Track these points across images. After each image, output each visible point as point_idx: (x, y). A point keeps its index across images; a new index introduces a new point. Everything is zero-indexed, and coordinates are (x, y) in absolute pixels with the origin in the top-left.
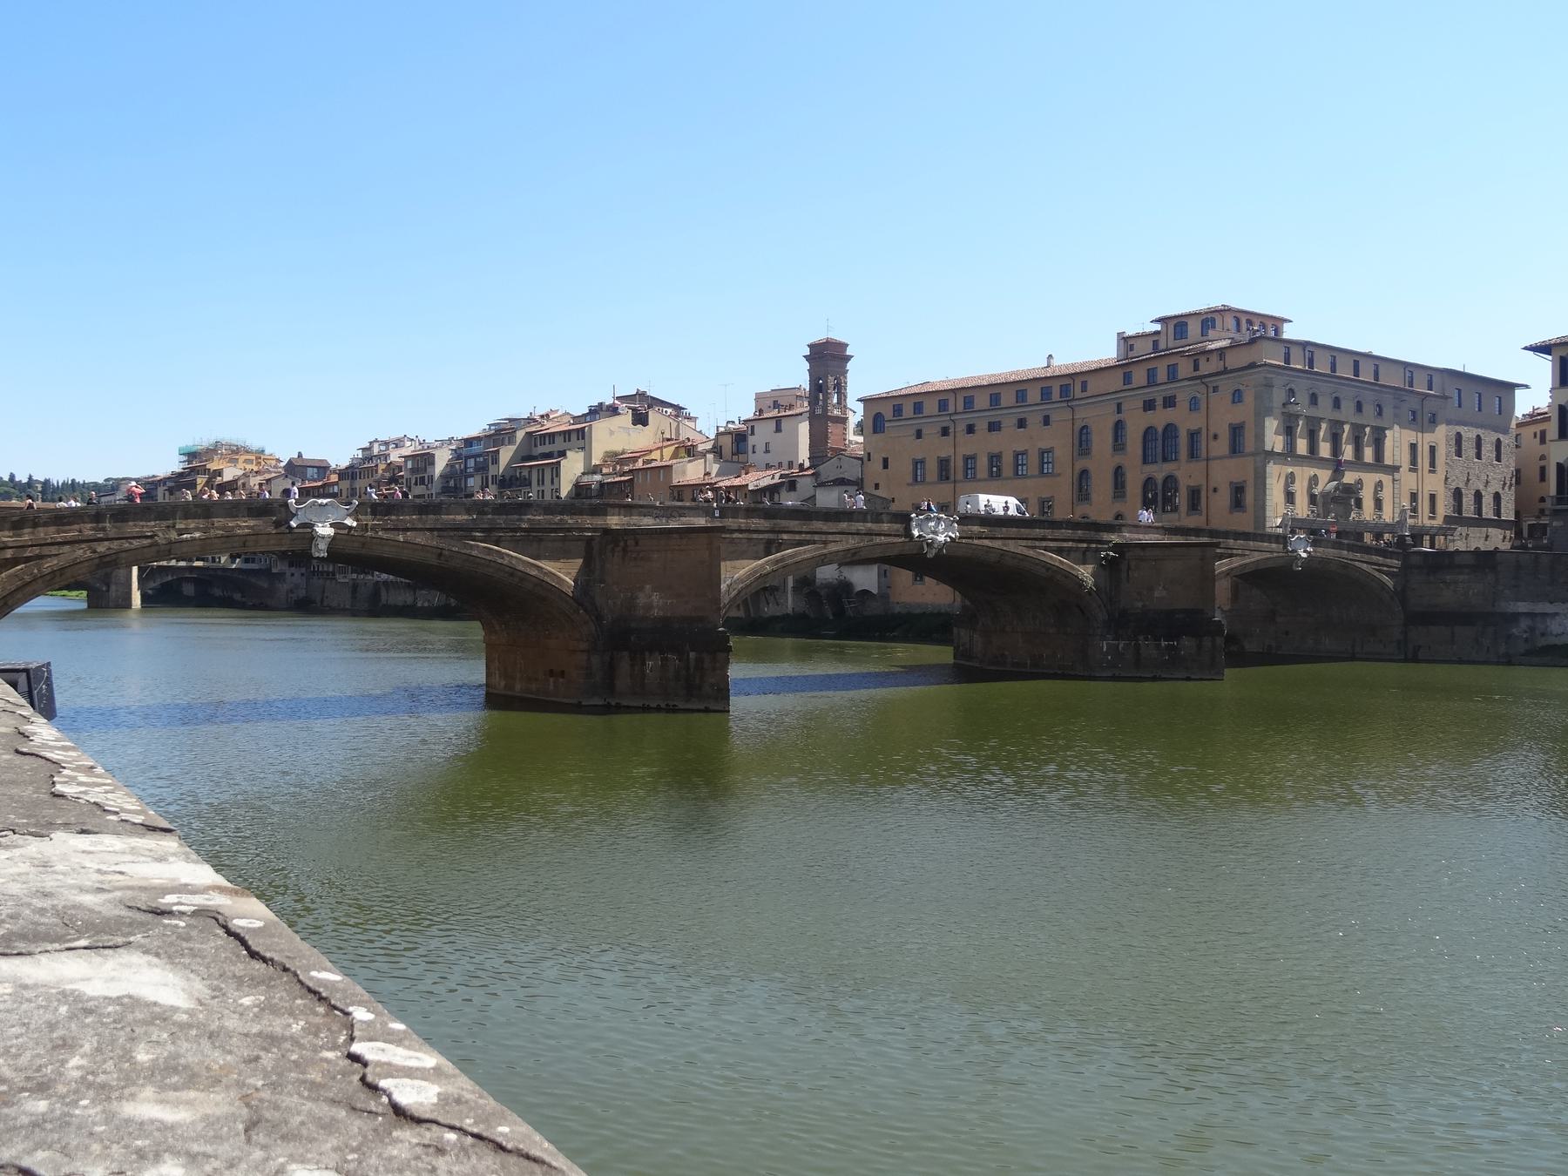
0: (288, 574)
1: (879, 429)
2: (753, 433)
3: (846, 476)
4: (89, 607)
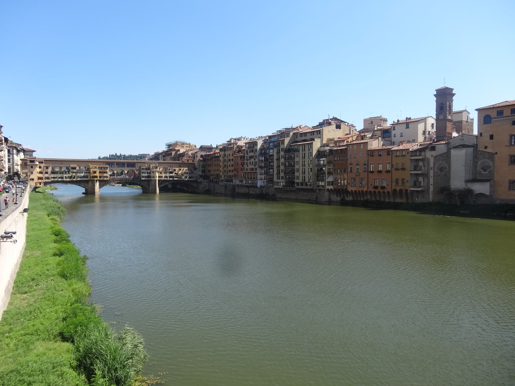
2: (394, 129)
4: (143, 193)
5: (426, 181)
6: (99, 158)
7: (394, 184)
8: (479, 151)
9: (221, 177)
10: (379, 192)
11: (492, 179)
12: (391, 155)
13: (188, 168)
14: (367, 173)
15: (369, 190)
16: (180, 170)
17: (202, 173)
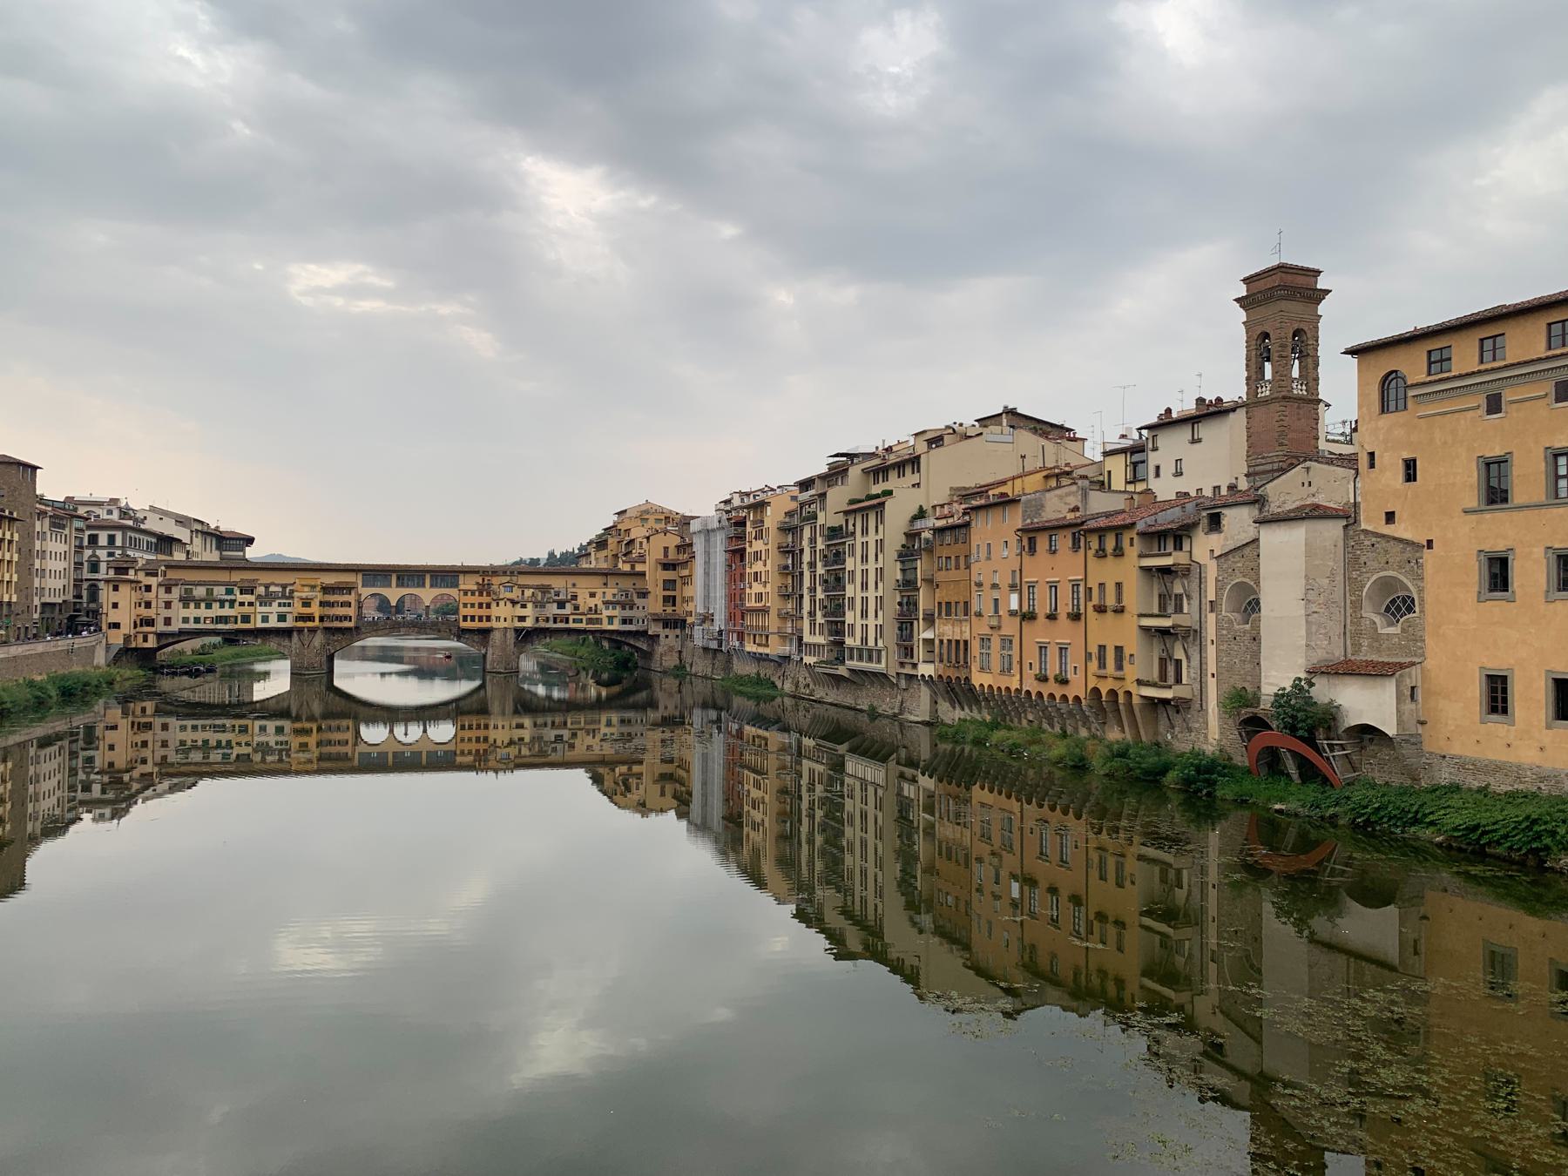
0: (662, 638)
1: (1392, 405)
2: (1155, 449)
3: (1320, 500)
5: (1195, 662)
6: (552, 555)
7: (1093, 666)
8: (1366, 532)
10: (1052, 696)
11: (1413, 664)
12: (1082, 550)
14: (1018, 619)
15: (1025, 689)
16: (593, 595)
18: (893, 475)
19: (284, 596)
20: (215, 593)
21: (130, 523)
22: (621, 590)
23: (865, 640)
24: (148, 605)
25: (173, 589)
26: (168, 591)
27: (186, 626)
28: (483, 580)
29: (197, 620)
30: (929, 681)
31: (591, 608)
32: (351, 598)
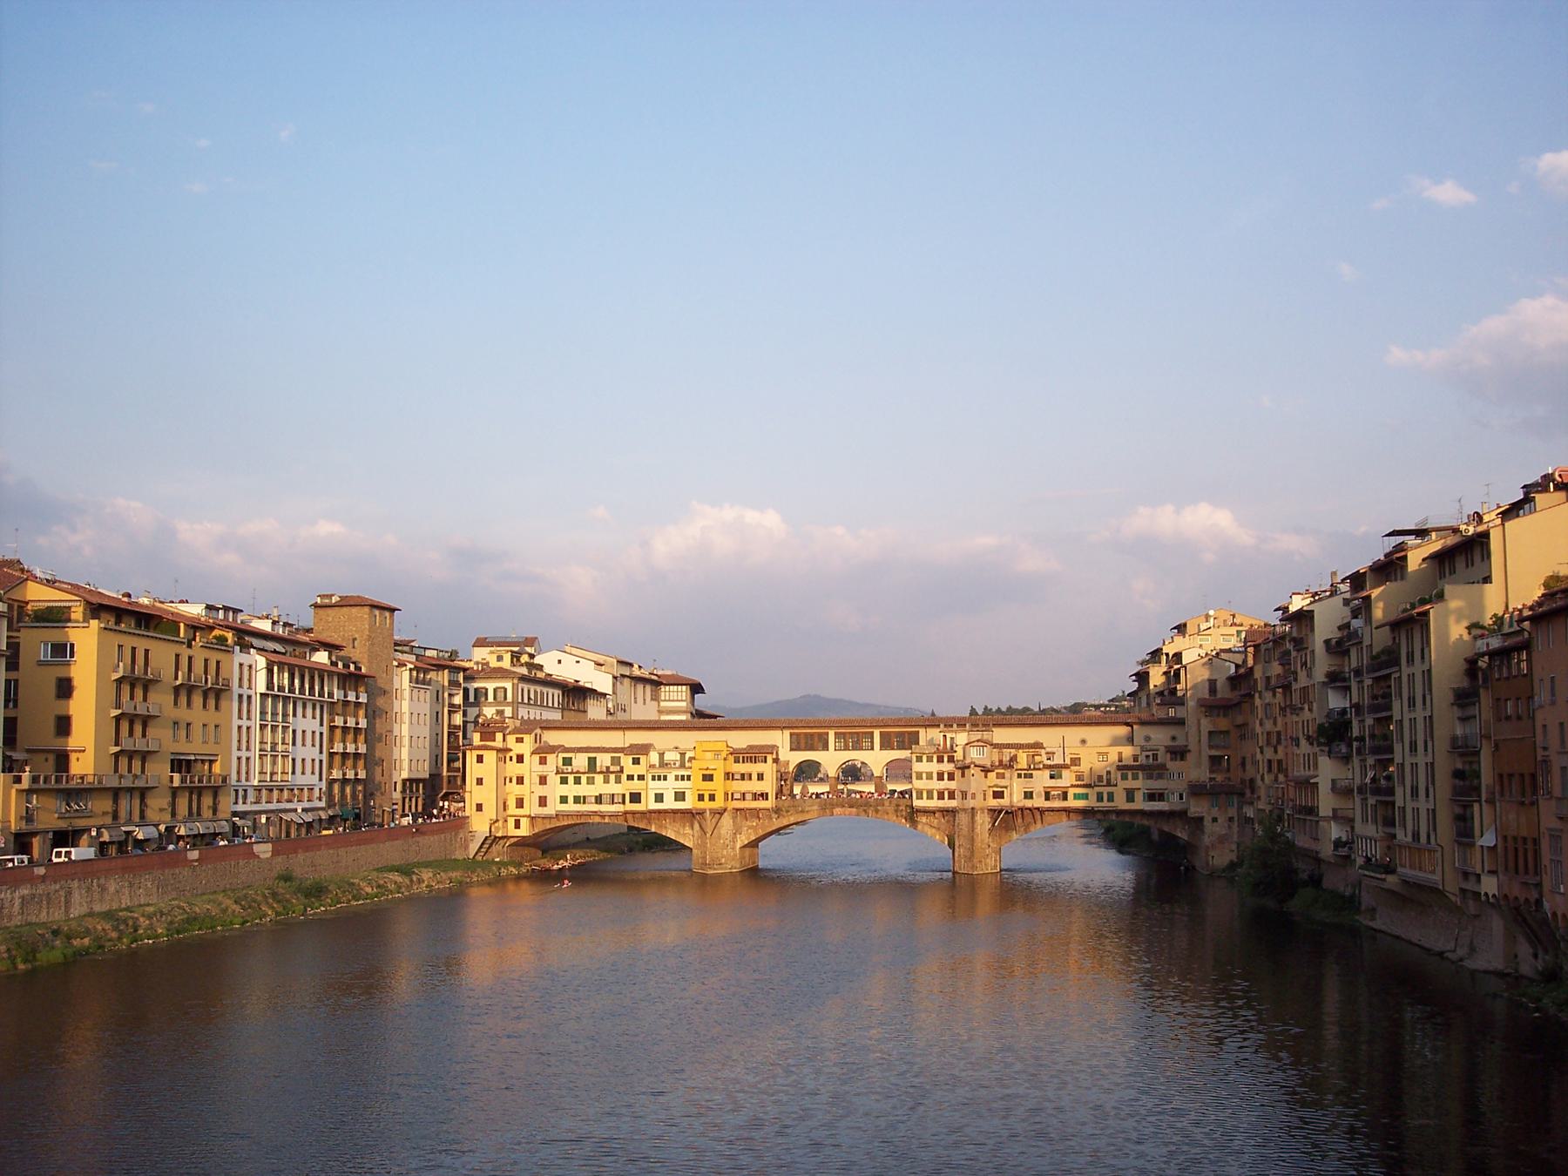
0: (1207, 822)
9: (1259, 798)
13: (1142, 751)
17: (1211, 772)
18: (1460, 563)
19: (683, 766)
20: (598, 764)
21: (524, 671)
22: (1143, 749)
23: (1416, 836)
24: (520, 780)
25: (551, 758)
26: (543, 761)
27: (564, 807)
28: (945, 736)
29: (577, 800)
30: (1501, 903)
31: (1100, 778)
32: (768, 768)
